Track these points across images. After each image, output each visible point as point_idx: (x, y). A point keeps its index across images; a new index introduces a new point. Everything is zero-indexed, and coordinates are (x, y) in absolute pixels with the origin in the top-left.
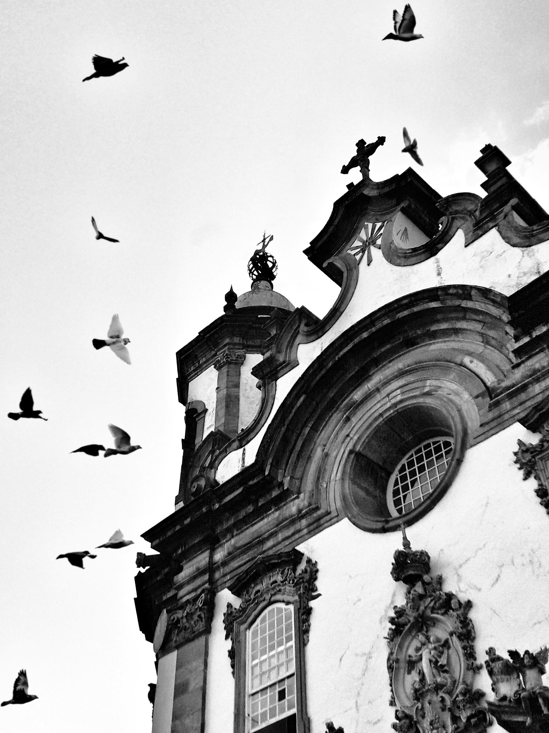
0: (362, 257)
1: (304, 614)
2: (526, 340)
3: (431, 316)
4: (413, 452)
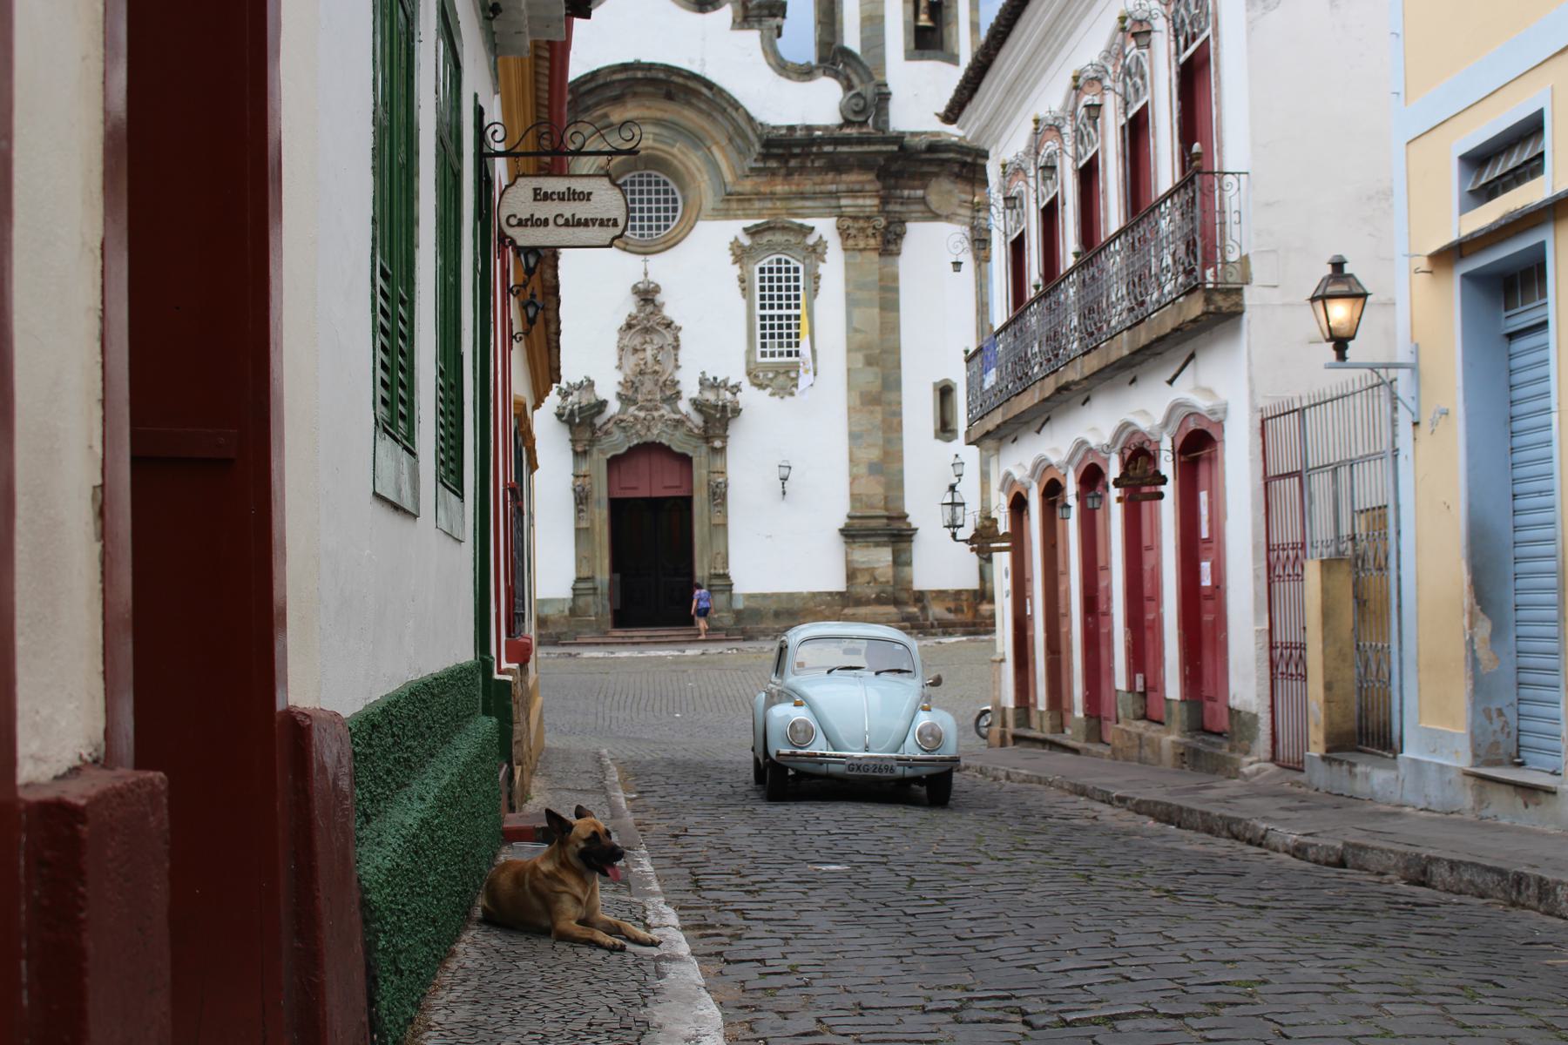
3: (698, 94)
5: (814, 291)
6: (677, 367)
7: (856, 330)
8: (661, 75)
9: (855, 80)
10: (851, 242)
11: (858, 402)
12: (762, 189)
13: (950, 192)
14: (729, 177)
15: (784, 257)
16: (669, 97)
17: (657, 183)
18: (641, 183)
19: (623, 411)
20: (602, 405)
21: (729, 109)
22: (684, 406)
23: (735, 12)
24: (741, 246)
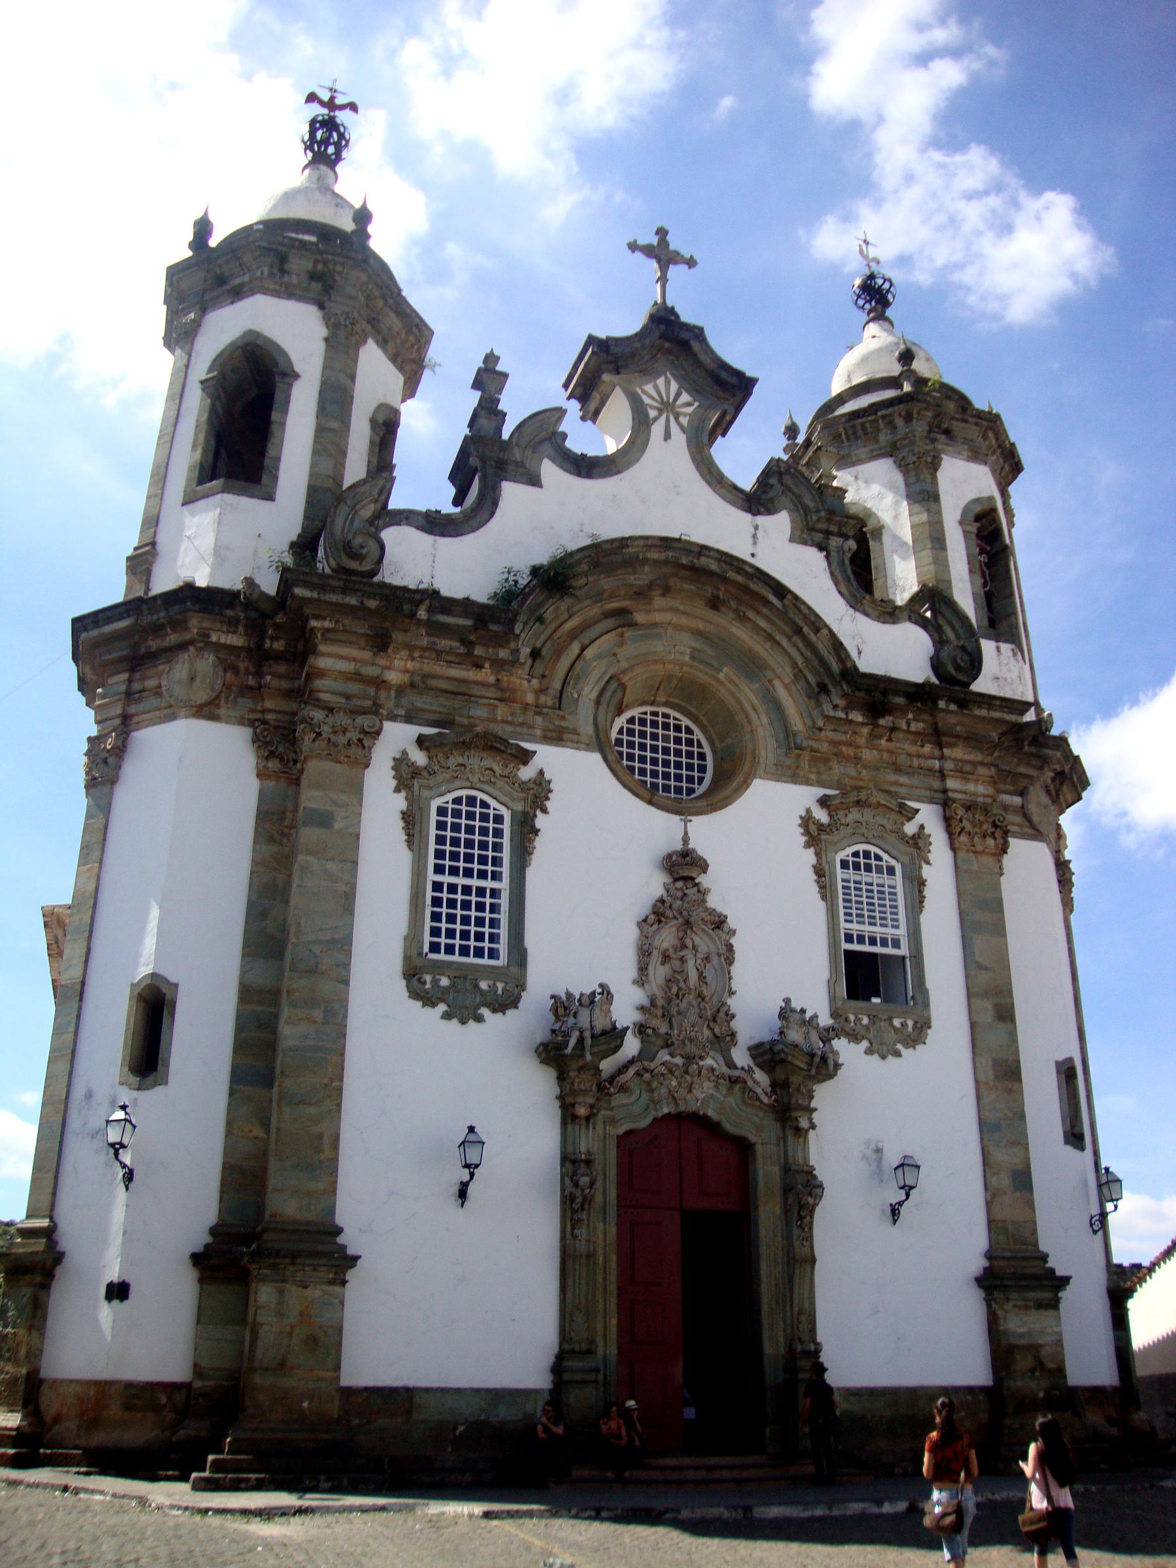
0: (656, 419)
1: (526, 830)
2: (842, 715)
4: (649, 709)
5: (917, 901)
6: (731, 993)
7: (981, 967)
8: (714, 566)
9: (949, 633)
10: (964, 838)
11: (991, 1075)
13: (1046, 807)
14: (797, 723)
15: (873, 849)
16: (714, 604)
20: (613, 1036)
21: (806, 629)
23: (792, 522)
24: (821, 827)
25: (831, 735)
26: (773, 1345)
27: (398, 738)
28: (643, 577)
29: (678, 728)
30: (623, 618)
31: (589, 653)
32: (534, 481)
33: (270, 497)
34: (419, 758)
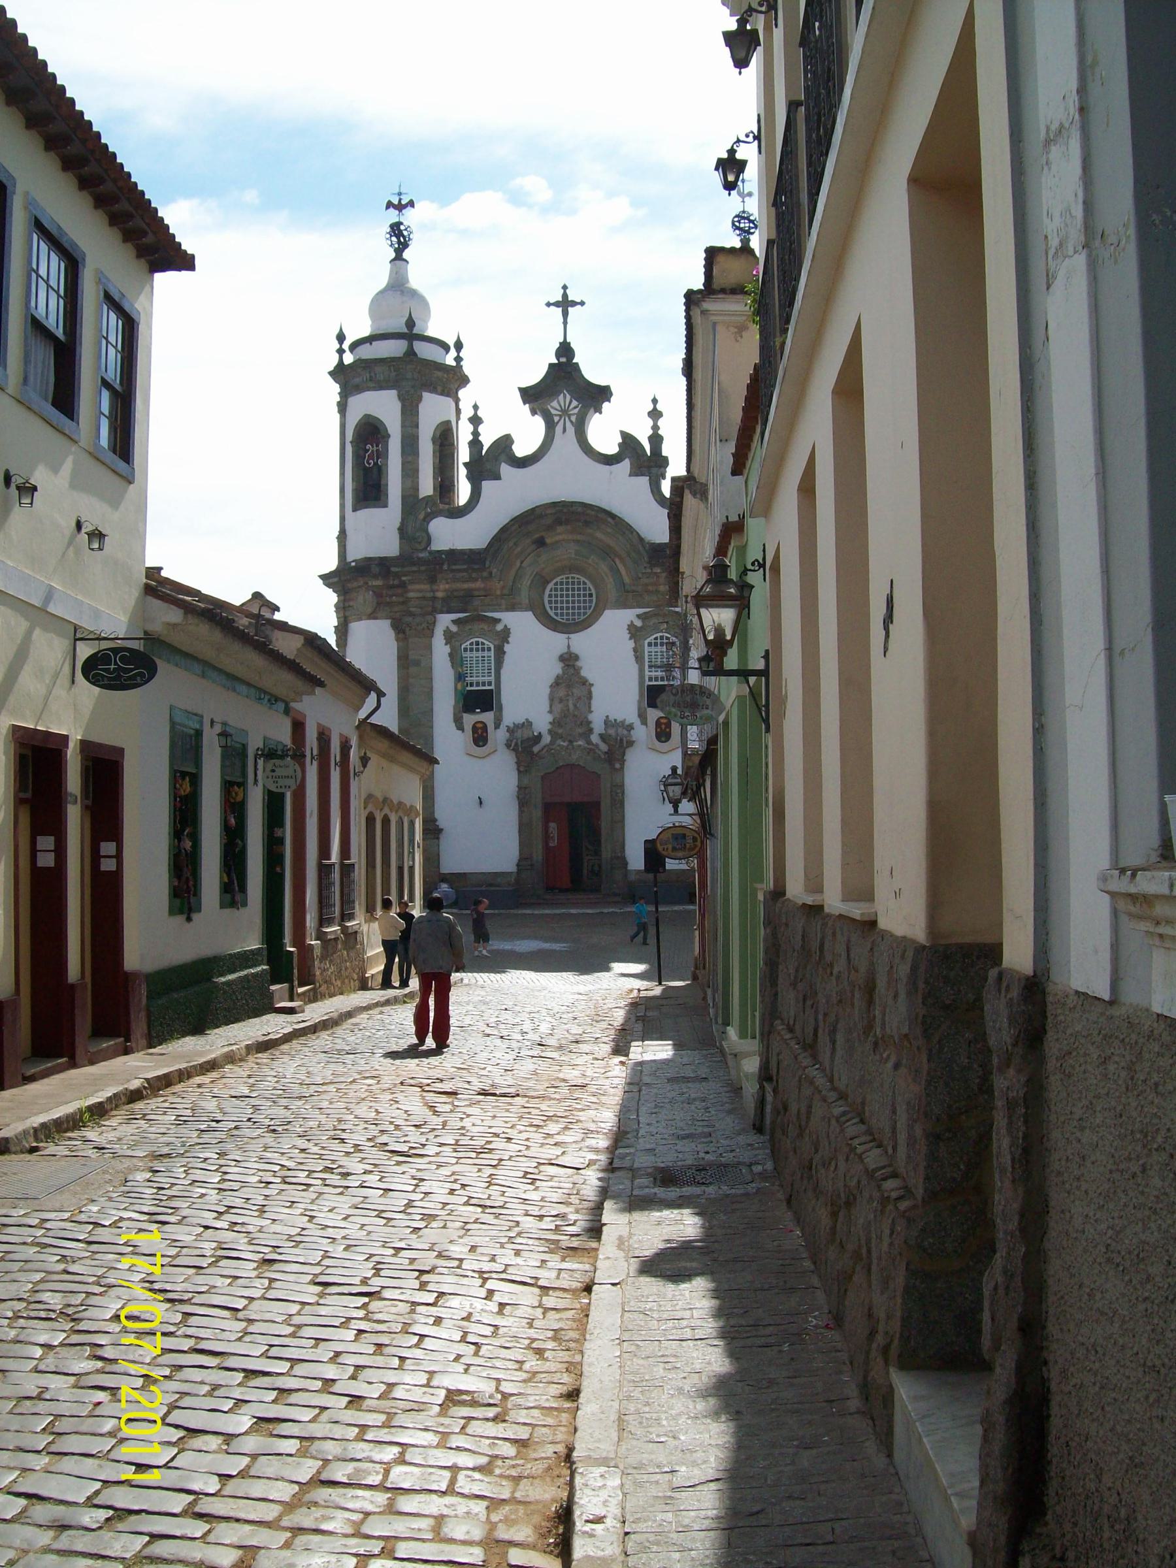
1: (500, 653)
8: (580, 509)
12: (650, 588)
14: (627, 580)
17: (579, 583)
18: (567, 583)
19: (552, 743)
20: (540, 736)
22: (595, 738)
25: (646, 581)
26: (606, 853)
27: (445, 621)
28: (549, 521)
29: (579, 583)
30: (541, 543)
31: (524, 564)
32: (498, 477)
33: (386, 506)
34: (454, 629)
